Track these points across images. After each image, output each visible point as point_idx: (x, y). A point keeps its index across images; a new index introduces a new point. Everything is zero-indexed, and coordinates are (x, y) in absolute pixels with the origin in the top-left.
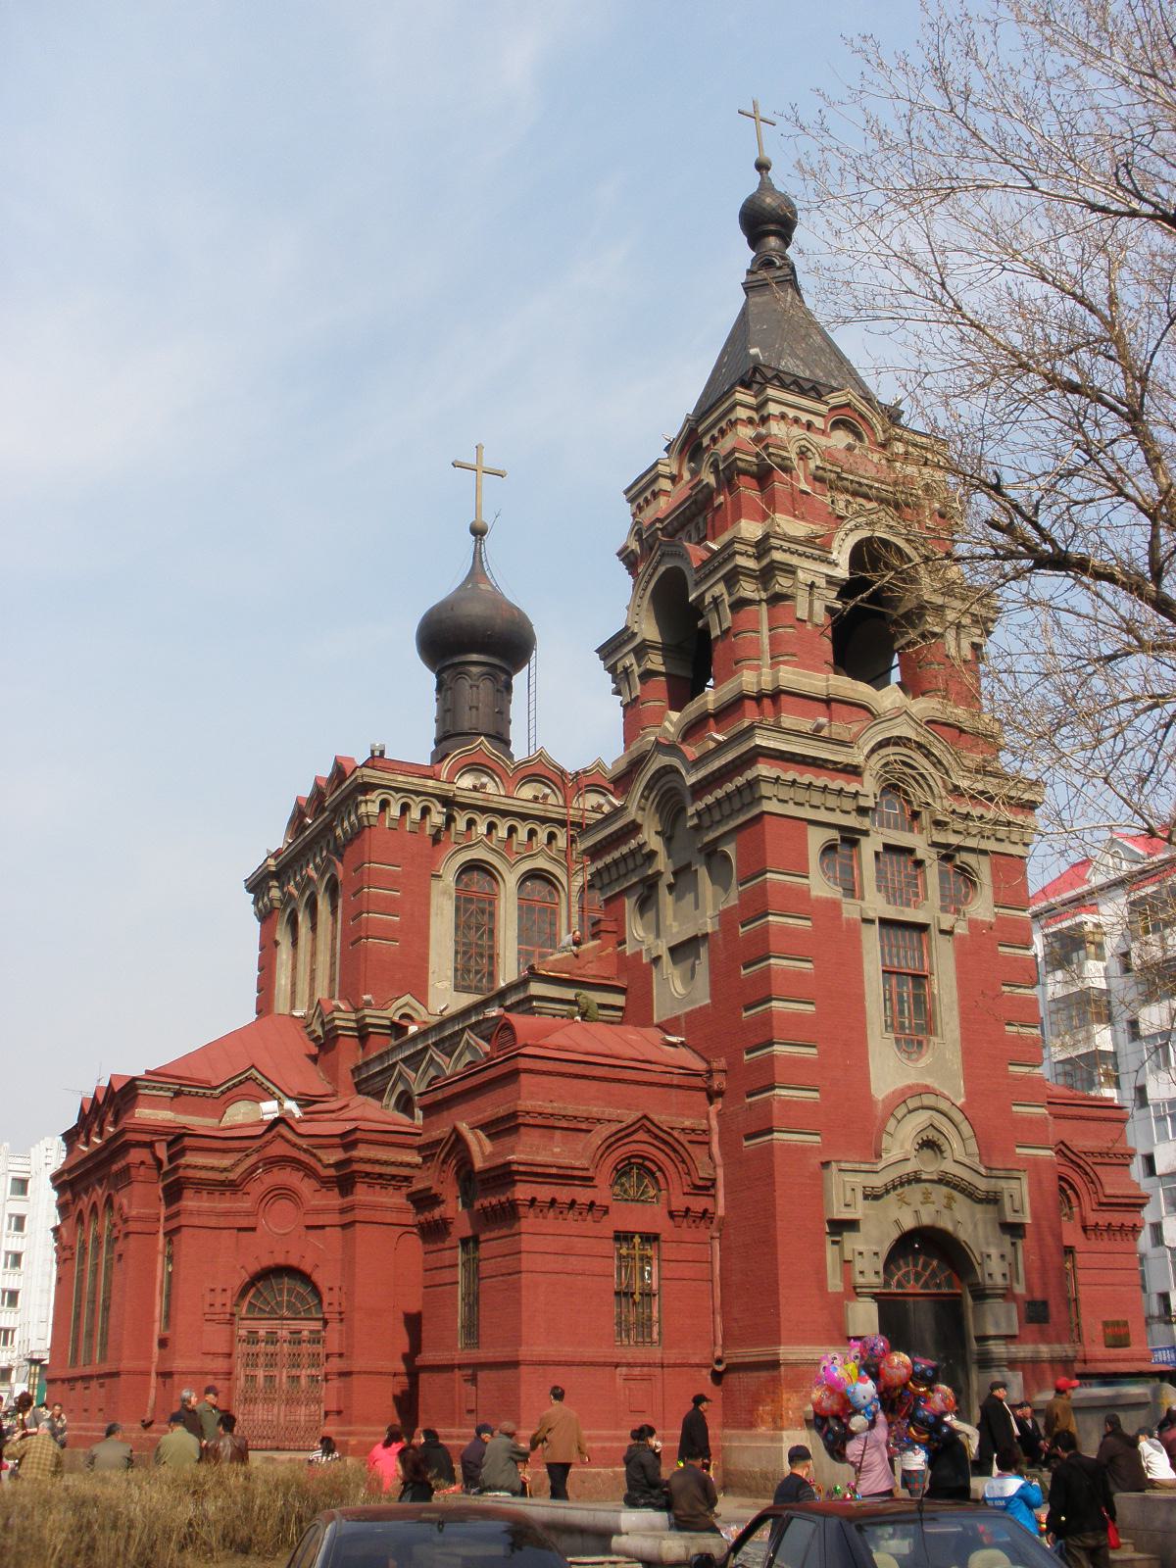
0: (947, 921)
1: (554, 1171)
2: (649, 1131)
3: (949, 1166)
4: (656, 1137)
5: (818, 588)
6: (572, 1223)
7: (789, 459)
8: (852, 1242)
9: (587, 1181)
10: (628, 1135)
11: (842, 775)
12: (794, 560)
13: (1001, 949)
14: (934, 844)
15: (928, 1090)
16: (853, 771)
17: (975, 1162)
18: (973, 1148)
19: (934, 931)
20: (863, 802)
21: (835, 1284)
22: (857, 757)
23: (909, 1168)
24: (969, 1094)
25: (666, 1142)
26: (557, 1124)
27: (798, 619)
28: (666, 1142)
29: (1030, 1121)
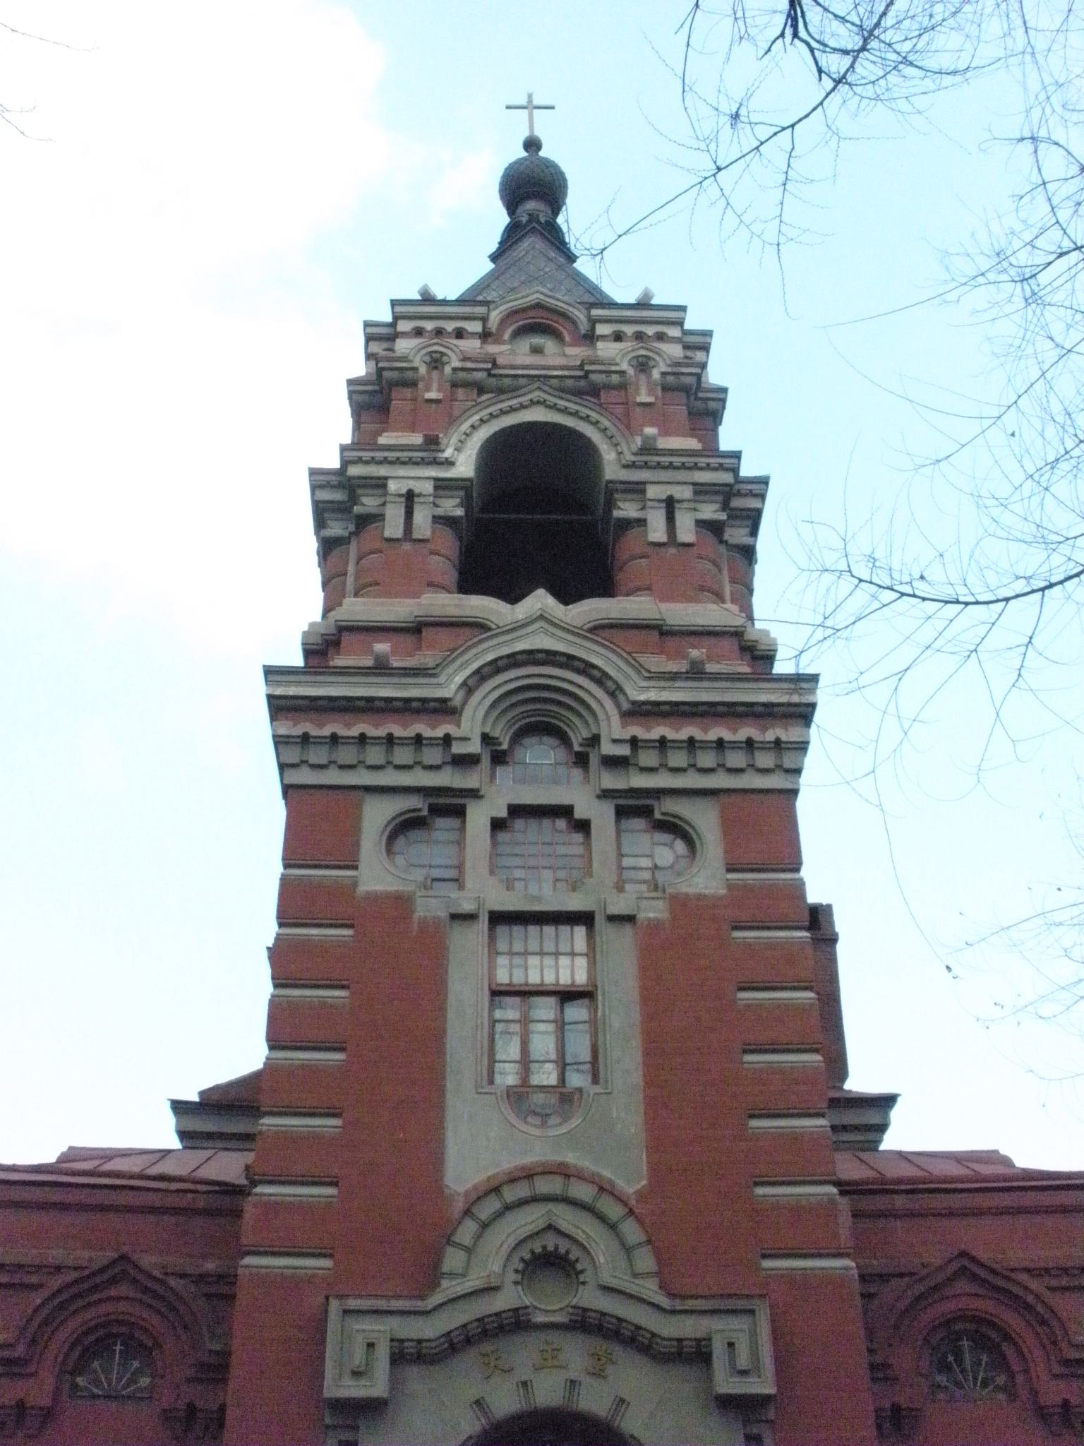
0: (619, 906)
2: (135, 1281)
3: (590, 1298)
4: (146, 1290)
7: (415, 369)
10: (95, 1289)
12: (382, 471)
14: (606, 794)
15: (564, 1171)
16: (443, 709)
17: (650, 1289)
18: (645, 1261)
19: (599, 921)
20: (457, 749)
22: (448, 686)
23: (502, 1302)
24: (655, 1171)
25: (155, 1295)
27: (389, 540)
28: (155, 1295)
29: (797, 1211)
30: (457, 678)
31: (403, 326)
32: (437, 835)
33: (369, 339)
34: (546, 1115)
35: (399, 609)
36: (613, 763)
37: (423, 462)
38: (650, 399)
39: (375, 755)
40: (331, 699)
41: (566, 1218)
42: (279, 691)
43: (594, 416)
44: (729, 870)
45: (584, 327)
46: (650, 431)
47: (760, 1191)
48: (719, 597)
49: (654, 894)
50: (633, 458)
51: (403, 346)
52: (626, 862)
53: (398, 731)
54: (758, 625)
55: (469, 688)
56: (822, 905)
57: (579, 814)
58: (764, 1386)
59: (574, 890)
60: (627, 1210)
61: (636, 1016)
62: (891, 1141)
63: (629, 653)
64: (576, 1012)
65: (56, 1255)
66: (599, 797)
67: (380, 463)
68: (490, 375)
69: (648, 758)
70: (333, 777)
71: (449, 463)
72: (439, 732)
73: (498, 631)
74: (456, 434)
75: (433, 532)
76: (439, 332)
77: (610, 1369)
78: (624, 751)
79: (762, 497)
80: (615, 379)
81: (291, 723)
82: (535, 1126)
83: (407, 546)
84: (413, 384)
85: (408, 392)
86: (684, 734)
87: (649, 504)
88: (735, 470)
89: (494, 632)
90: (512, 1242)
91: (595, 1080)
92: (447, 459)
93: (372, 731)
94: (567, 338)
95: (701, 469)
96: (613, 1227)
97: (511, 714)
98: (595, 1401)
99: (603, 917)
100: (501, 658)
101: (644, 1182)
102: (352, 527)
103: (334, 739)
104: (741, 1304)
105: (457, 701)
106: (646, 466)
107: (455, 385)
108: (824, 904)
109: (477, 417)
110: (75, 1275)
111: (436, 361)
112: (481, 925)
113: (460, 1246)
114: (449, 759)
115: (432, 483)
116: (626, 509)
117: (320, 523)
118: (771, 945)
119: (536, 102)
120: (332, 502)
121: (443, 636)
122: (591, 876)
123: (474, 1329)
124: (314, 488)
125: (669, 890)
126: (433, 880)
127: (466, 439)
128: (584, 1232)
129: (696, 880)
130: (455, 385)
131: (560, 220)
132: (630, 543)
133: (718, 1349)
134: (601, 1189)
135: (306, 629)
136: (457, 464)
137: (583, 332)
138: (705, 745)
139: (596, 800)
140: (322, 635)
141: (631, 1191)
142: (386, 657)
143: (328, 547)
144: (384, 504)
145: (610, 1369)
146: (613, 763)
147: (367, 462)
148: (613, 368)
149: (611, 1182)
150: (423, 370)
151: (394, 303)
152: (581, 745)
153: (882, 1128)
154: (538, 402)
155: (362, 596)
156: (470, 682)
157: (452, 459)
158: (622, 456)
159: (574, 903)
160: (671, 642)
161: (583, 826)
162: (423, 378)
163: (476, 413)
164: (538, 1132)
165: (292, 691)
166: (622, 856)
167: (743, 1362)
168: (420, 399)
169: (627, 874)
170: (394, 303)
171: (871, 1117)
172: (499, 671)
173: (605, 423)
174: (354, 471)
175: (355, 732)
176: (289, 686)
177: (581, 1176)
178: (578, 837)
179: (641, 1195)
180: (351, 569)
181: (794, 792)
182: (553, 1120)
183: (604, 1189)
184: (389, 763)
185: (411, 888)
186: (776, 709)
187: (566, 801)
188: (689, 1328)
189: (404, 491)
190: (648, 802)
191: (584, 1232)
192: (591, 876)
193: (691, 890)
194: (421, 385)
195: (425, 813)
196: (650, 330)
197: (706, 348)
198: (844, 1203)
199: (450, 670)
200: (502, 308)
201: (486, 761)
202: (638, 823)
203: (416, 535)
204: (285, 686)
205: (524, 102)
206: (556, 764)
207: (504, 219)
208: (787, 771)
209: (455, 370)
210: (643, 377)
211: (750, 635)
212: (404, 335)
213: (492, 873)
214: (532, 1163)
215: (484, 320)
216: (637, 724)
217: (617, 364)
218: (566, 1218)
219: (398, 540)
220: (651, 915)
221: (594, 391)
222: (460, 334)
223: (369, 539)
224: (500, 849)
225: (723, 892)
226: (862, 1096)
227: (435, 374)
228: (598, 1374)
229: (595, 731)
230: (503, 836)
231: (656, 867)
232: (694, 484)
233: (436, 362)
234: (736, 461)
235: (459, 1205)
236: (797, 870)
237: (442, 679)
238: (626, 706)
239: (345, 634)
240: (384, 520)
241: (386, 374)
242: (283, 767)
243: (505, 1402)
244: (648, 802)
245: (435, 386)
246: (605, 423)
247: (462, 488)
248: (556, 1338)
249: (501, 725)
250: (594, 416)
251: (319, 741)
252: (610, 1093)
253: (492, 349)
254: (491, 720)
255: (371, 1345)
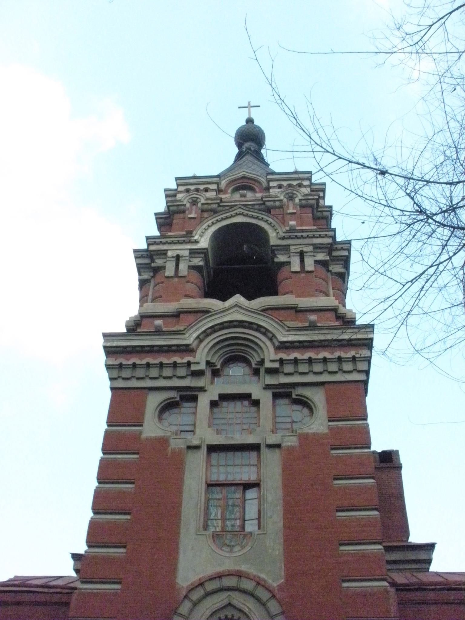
0: (272, 439)
5: (182, 257)
11: (178, 354)
12: (165, 247)
14: (267, 387)
15: (239, 575)
16: (188, 349)
19: (263, 449)
20: (193, 368)
22: (190, 338)
30: (194, 335)
31: (181, 188)
32: (183, 410)
33: (167, 196)
34: (233, 546)
35: (170, 307)
36: (271, 372)
37: (184, 242)
38: (295, 211)
39: (154, 372)
40: (134, 347)
41: (238, 599)
42: (108, 344)
43: (266, 218)
44: (329, 421)
45: (265, 184)
46: (292, 223)
47: (345, 585)
48: (327, 295)
49: (292, 434)
50: (284, 235)
51: (179, 196)
52: (278, 420)
53: (165, 361)
54: (348, 307)
55: (200, 339)
56: (393, 451)
57: (254, 397)
59: (251, 433)
60: (271, 595)
62: (433, 568)
63: (281, 321)
64: (251, 494)
66: (264, 389)
67: (164, 244)
68: (219, 206)
69: (289, 368)
70: (135, 384)
71: (197, 242)
72: (185, 360)
73: (215, 312)
74: (200, 229)
75: (188, 274)
76: (197, 190)
78: (276, 365)
79: (349, 250)
80: (278, 203)
81: (114, 359)
82: (227, 552)
83: (176, 280)
84: (184, 212)
85: (181, 216)
86: (306, 356)
87: (292, 254)
88: (334, 237)
89: (213, 313)
90: (208, 613)
91: (259, 528)
92: (195, 240)
93: (152, 361)
94: (257, 190)
95: (317, 237)
96: (263, 604)
97: (222, 351)
99: (265, 445)
100: (216, 325)
101: (282, 581)
102: (152, 274)
103: (134, 365)
105: (194, 346)
106: (290, 238)
107: (203, 211)
108: (395, 450)
109: (210, 222)
111: (194, 201)
112: (202, 451)
114: (189, 373)
115: (188, 251)
116: (281, 258)
117: (140, 274)
118: (351, 456)
119: (252, 104)
120: (144, 264)
121: (191, 317)
122: (259, 426)
124: (136, 258)
126: (181, 431)
127: (205, 232)
128: (248, 607)
129: (312, 426)
130: (203, 211)
131: (263, 151)
132: (283, 274)
134: (258, 584)
135: (128, 319)
136: (201, 242)
137: (264, 187)
138: (317, 361)
139: (263, 391)
140: (134, 321)
141: (275, 585)
142: (160, 326)
143: (143, 284)
144: (166, 262)
146: (271, 372)
147: (158, 244)
148: (277, 199)
149: (265, 581)
150: (188, 205)
151: (177, 179)
152: (256, 365)
153: (429, 561)
154: (240, 214)
155: (154, 302)
156: (201, 337)
157: (198, 240)
158: (278, 234)
159: (251, 439)
160: (301, 315)
161: (256, 403)
162: (188, 209)
163: (210, 220)
164: (228, 555)
165: (115, 344)
166: (276, 417)
168: (186, 218)
169: (278, 426)
170: (177, 179)
171: (422, 556)
172: (215, 331)
173: (271, 220)
174: (152, 248)
175: (144, 362)
176: (113, 342)
177: (248, 577)
178: (254, 409)
179: (281, 588)
180: (150, 293)
184: (160, 376)
185: (169, 434)
186: (353, 342)
187: (248, 391)
189: (175, 255)
190: (289, 390)
191: (248, 607)
192: (259, 426)
193: (310, 431)
194: (187, 212)
195: (178, 399)
198: (392, 590)
199: (191, 331)
200: (226, 180)
201: (208, 374)
202: (286, 401)
203: (179, 275)
204: (112, 342)
205: (246, 105)
206: (244, 375)
207: (236, 150)
209: (203, 204)
211: (341, 310)
212: (181, 192)
213: (210, 426)
214: (223, 571)
215: (218, 184)
216: (283, 353)
217: (278, 197)
218: (238, 599)
219: (171, 277)
220: (289, 444)
221: (268, 210)
222: (206, 190)
223: (159, 277)
224: (216, 416)
226: (415, 544)
227: (194, 207)
229: (262, 357)
230: (216, 410)
231: (294, 422)
232: (314, 245)
233: (194, 202)
234: (333, 233)
235: (184, 593)
236: (366, 419)
237: (187, 335)
238: (277, 344)
239: (144, 319)
240: (165, 269)
241: (171, 208)
242: (111, 379)
244: (289, 390)
245: (194, 212)
246: (271, 220)
247: (202, 253)
249: (217, 356)
250: (266, 218)
251: (127, 367)
252: (265, 534)
253: (222, 196)
254: (212, 353)
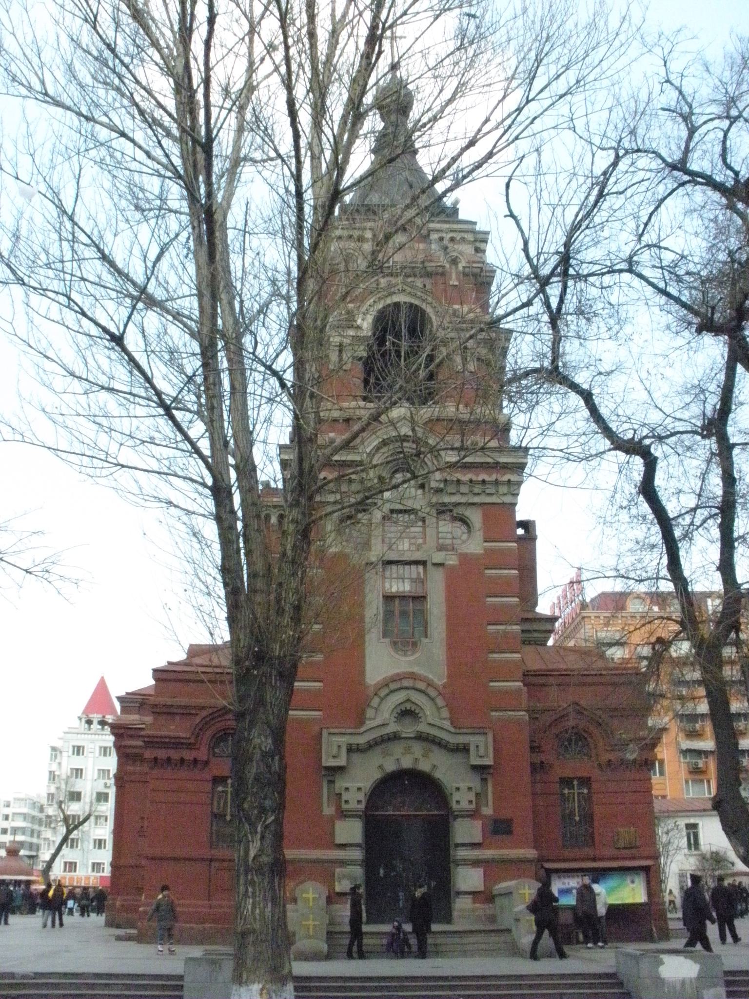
0: (438, 557)
1: (167, 740)
3: (423, 728)
6: (184, 773)
8: (341, 783)
9: (190, 746)
13: (487, 571)
15: (413, 676)
17: (447, 724)
18: (445, 713)
21: (328, 810)
26: (175, 711)
29: (506, 692)
38: (456, 283)
44: (485, 541)
58: (489, 761)
61: (444, 609)
65: (201, 701)
69: (451, 489)
71: (359, 328)
77: (431, 755)
80: (440, 270)
96: (433, 699)
98: (424, 766)
104: (482, 731)
109: (372, 300)
110: (210, 711)
113: (372, 707)
118: (500, 577)
123: (379, 740)
125: (459, 551)
133: (472, 749)
145: (431, 755)
159: (417, 556)
164: (404, 659)
167: (482, 751)
179: (444, 686)
181: (515, 504)
182: (409, 653)
183: (430, 684)
188: (461, 739)
193: (469, 551)
196: (458, 236)
197: (485, 241)
198: (525, 688)
208: (513, 495)
210: (454, 267)
225: (482, 552)
228: (425, 756)
243: (390, 767)
248: (410, 743)
255: (339, 746)
